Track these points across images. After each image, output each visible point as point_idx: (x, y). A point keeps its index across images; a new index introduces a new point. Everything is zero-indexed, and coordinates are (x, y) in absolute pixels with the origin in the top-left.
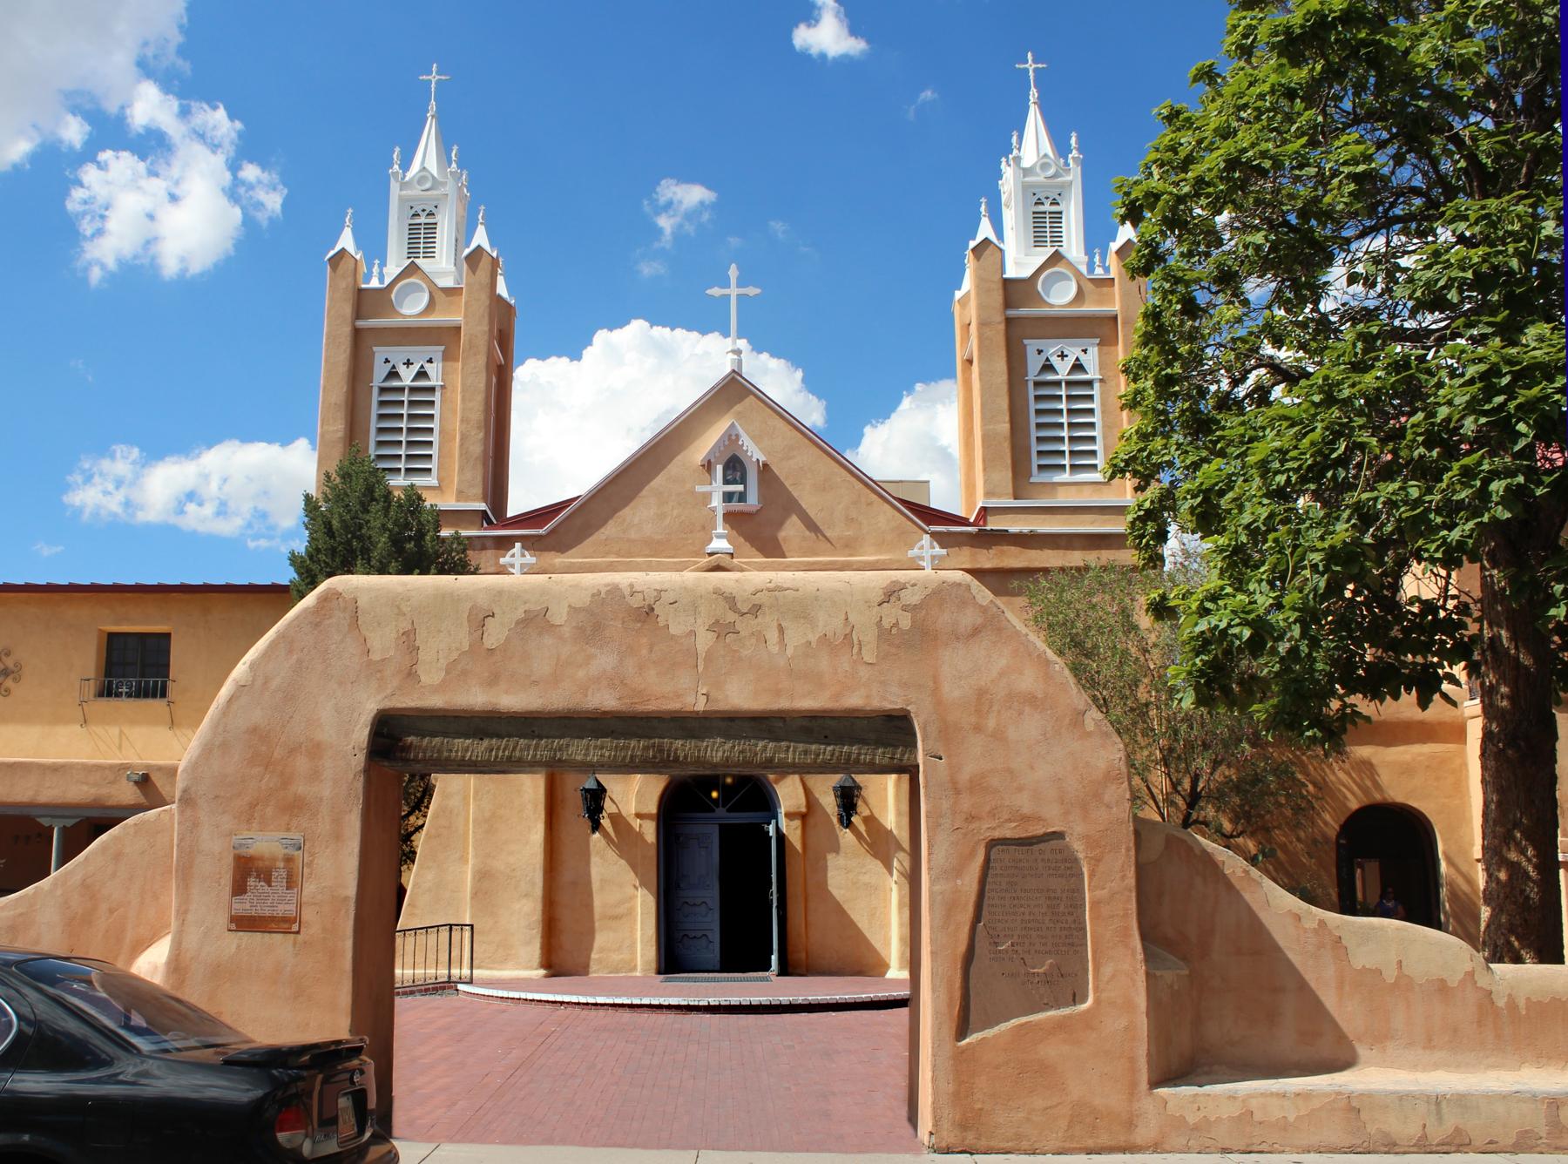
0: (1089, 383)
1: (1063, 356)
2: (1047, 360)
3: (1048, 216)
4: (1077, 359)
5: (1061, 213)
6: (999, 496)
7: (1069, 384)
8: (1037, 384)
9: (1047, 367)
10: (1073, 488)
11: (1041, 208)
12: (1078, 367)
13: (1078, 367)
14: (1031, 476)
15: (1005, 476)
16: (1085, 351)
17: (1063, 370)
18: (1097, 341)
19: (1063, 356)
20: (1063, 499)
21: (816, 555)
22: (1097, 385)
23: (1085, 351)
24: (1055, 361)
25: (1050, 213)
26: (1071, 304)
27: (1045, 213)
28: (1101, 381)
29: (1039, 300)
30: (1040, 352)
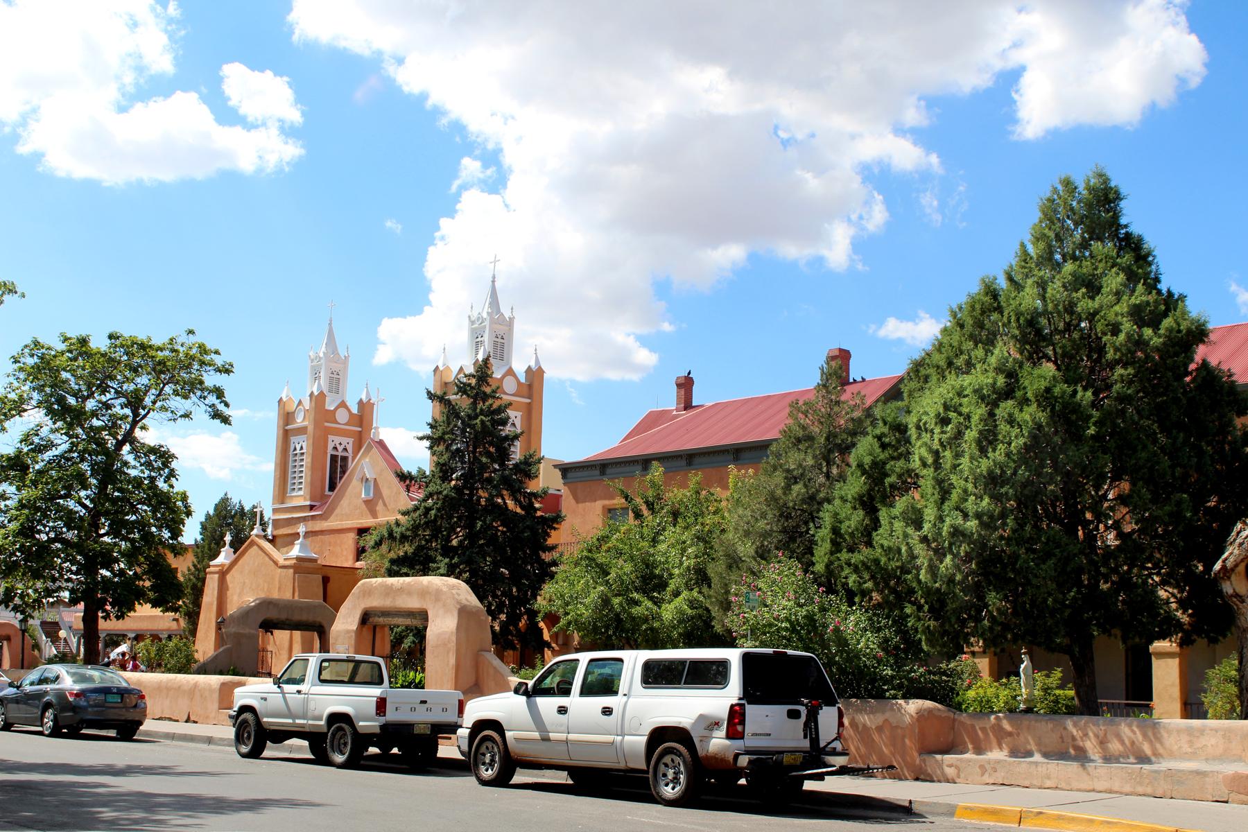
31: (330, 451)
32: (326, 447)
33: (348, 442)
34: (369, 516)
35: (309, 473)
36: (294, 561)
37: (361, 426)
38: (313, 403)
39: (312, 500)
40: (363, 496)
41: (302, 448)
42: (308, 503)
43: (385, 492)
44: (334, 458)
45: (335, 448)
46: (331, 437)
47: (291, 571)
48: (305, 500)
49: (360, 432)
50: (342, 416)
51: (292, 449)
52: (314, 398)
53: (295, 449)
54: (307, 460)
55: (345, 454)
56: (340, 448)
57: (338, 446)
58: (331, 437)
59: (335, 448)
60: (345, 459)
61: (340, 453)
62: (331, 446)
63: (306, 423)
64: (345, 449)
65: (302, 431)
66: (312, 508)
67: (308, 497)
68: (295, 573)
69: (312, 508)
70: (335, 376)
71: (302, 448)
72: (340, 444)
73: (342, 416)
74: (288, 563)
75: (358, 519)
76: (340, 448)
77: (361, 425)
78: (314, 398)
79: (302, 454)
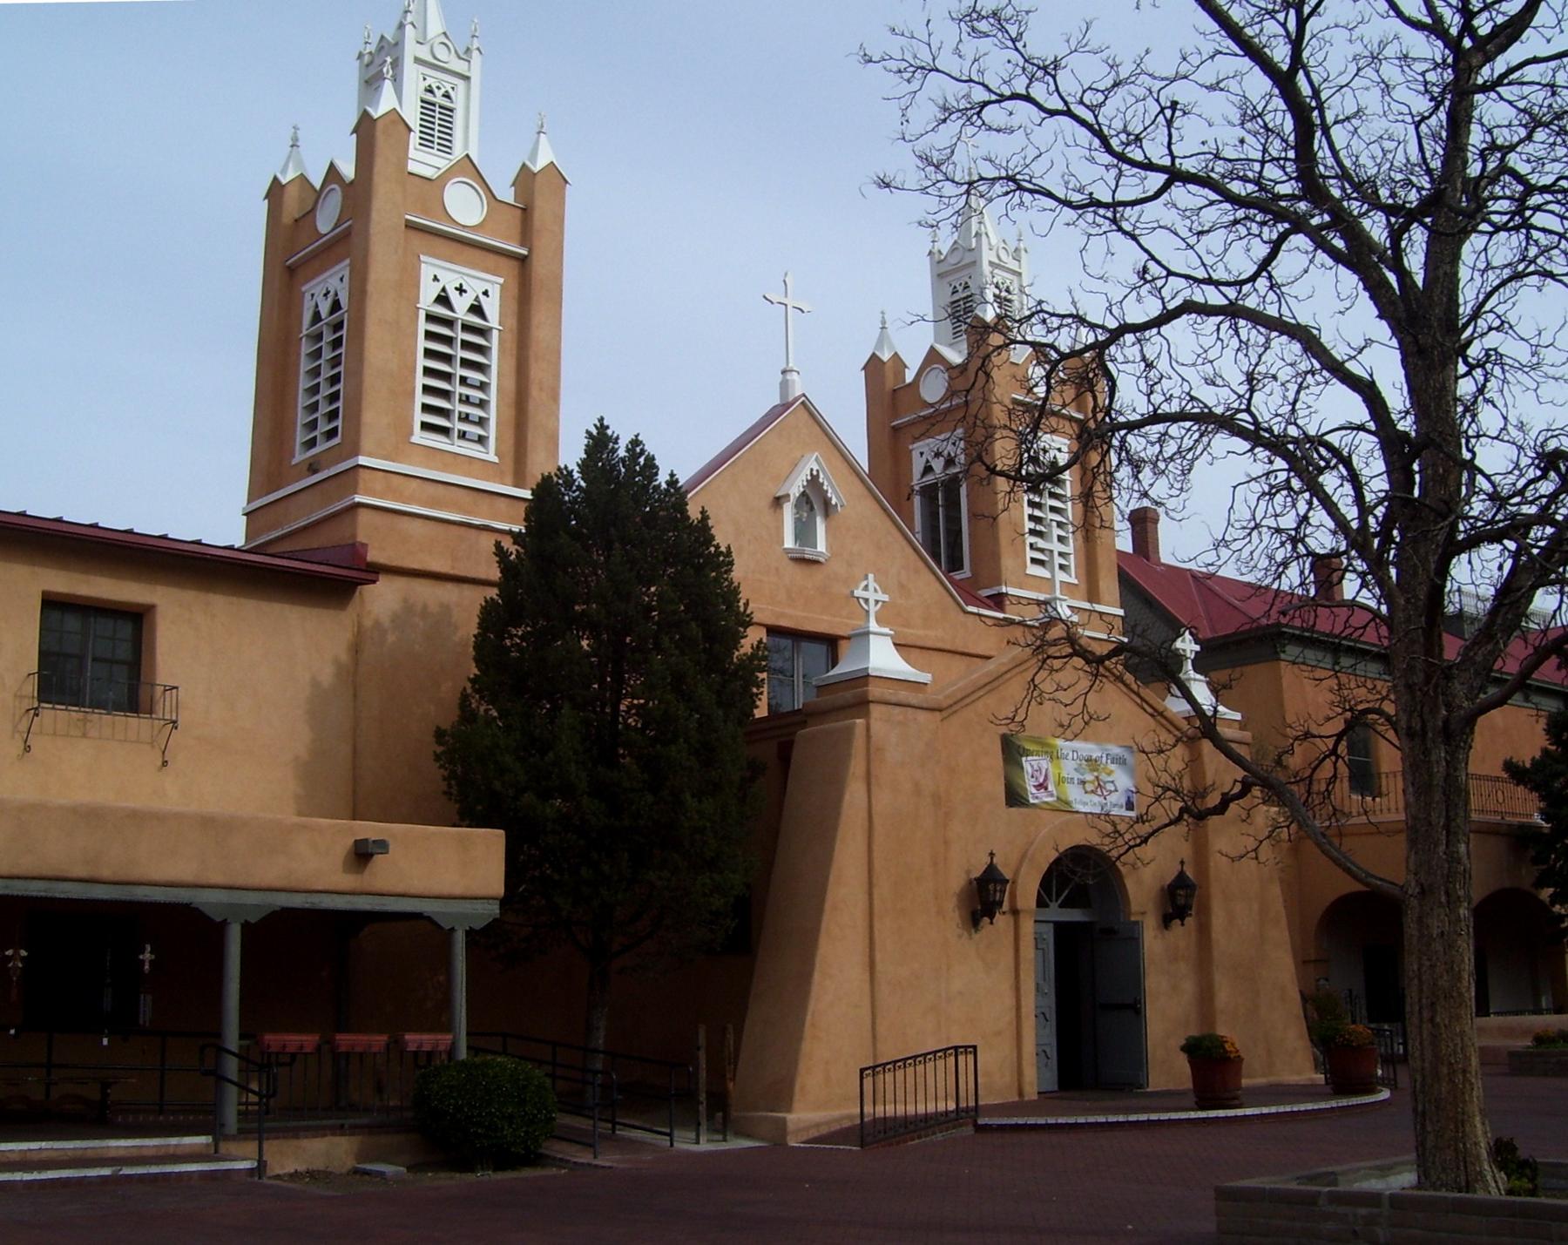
2: (444, 290)
3: (438, 109)
4: (477, 299)
5: (451, 110)
7: (467, 328)
8: (431, 318)
9: (443, 300)
11: (429, 97)
12: (476, 309)
13: (476, 309)
14: (411, 433)
19: (461, 290)
24: (454, 296)
25: (441, 107)
27: (434, 105)
30: (436, 279)
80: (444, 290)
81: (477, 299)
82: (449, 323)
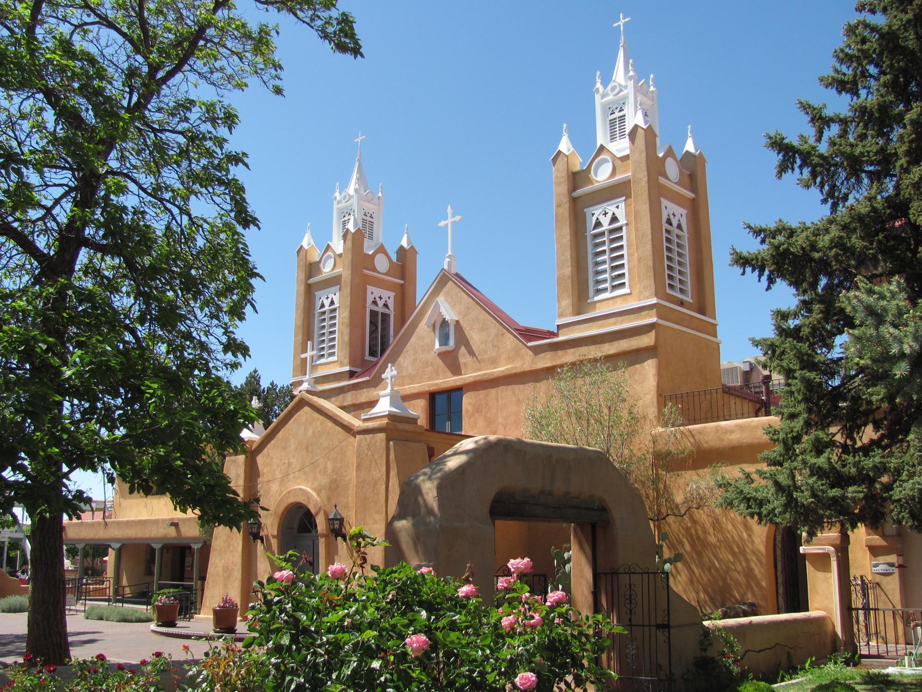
0: (620, 229)
1: (605, 214)
4: (614, 214)
6: (566, 316)
10: (611, 301)
12: (614, 219)
13: (614, 219)
15: (567, 302)
16: (617, 207)
17: (606, 221)
18: (624, 198)
20: (599, 311)
21: (480, 370)
22: (624, 228)
23: (617, 207)
26: (609, 178)
28: (627, 224)
29: (589, 181)
31: (369, 306)
32: (365, 300)
33: (389, 296)
34: (449, 373)
35: (347, 331)
36: (385, 421)
37: (402, 279)
38: (349, 243)
39: (351, 364)
40: (437, 346)
41: (332, 303)
42: (347, 368)
43: (475, 338)
44: (374, 314)
45: (375, 303)
46: (370, 289)
47: (382, 436)
48: (342, 365)
49: (402, 285)
50: (382, 264)
51: (318, 305)
52: (349, 237)
53: (323, 306)
54: (342, 317)
55: (385, 311)
56: (381, 303)
57: (378, 300)
58: (370, 289)
59: (375, 303)
60: (385, 317)
61: (380, 309)
62: (370, 299)
63: (339, 270)
64: (386, 305)
65: (334, 281)
66: (352, 374)
67: (346, 361)
68: (388, 440)
69: (352, 374)
70: (368, 219)
71: (332, 303)
72: (380, 298)
73: (382, 264)
74: (370, 425)
75: (429, 379)
76: (381, 303)
77: (403, 277)
78: (349, 237)
79: (335, 310)
80: (597, 219)
81: (614, 214)
82: (602, 234)
